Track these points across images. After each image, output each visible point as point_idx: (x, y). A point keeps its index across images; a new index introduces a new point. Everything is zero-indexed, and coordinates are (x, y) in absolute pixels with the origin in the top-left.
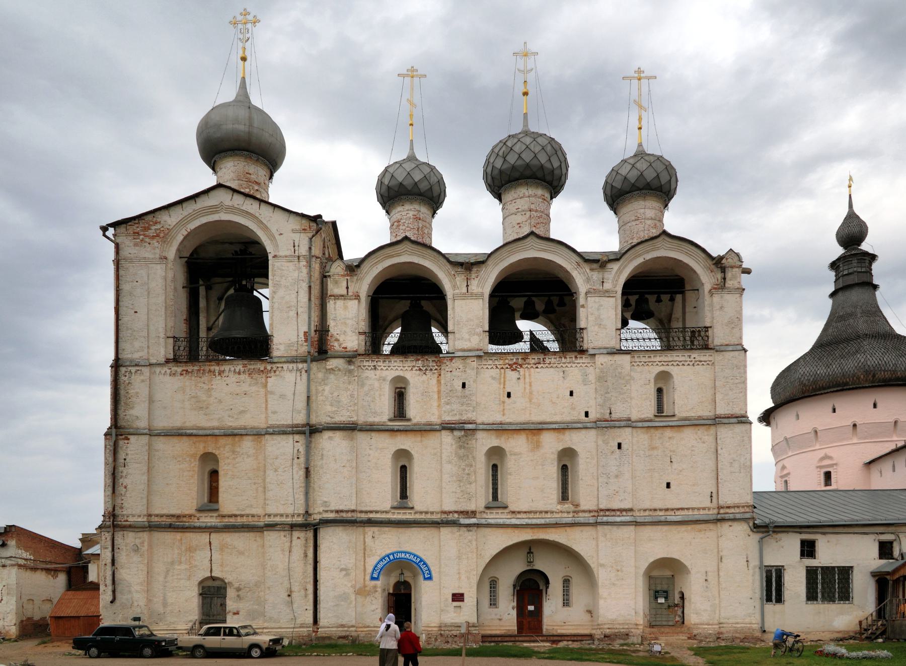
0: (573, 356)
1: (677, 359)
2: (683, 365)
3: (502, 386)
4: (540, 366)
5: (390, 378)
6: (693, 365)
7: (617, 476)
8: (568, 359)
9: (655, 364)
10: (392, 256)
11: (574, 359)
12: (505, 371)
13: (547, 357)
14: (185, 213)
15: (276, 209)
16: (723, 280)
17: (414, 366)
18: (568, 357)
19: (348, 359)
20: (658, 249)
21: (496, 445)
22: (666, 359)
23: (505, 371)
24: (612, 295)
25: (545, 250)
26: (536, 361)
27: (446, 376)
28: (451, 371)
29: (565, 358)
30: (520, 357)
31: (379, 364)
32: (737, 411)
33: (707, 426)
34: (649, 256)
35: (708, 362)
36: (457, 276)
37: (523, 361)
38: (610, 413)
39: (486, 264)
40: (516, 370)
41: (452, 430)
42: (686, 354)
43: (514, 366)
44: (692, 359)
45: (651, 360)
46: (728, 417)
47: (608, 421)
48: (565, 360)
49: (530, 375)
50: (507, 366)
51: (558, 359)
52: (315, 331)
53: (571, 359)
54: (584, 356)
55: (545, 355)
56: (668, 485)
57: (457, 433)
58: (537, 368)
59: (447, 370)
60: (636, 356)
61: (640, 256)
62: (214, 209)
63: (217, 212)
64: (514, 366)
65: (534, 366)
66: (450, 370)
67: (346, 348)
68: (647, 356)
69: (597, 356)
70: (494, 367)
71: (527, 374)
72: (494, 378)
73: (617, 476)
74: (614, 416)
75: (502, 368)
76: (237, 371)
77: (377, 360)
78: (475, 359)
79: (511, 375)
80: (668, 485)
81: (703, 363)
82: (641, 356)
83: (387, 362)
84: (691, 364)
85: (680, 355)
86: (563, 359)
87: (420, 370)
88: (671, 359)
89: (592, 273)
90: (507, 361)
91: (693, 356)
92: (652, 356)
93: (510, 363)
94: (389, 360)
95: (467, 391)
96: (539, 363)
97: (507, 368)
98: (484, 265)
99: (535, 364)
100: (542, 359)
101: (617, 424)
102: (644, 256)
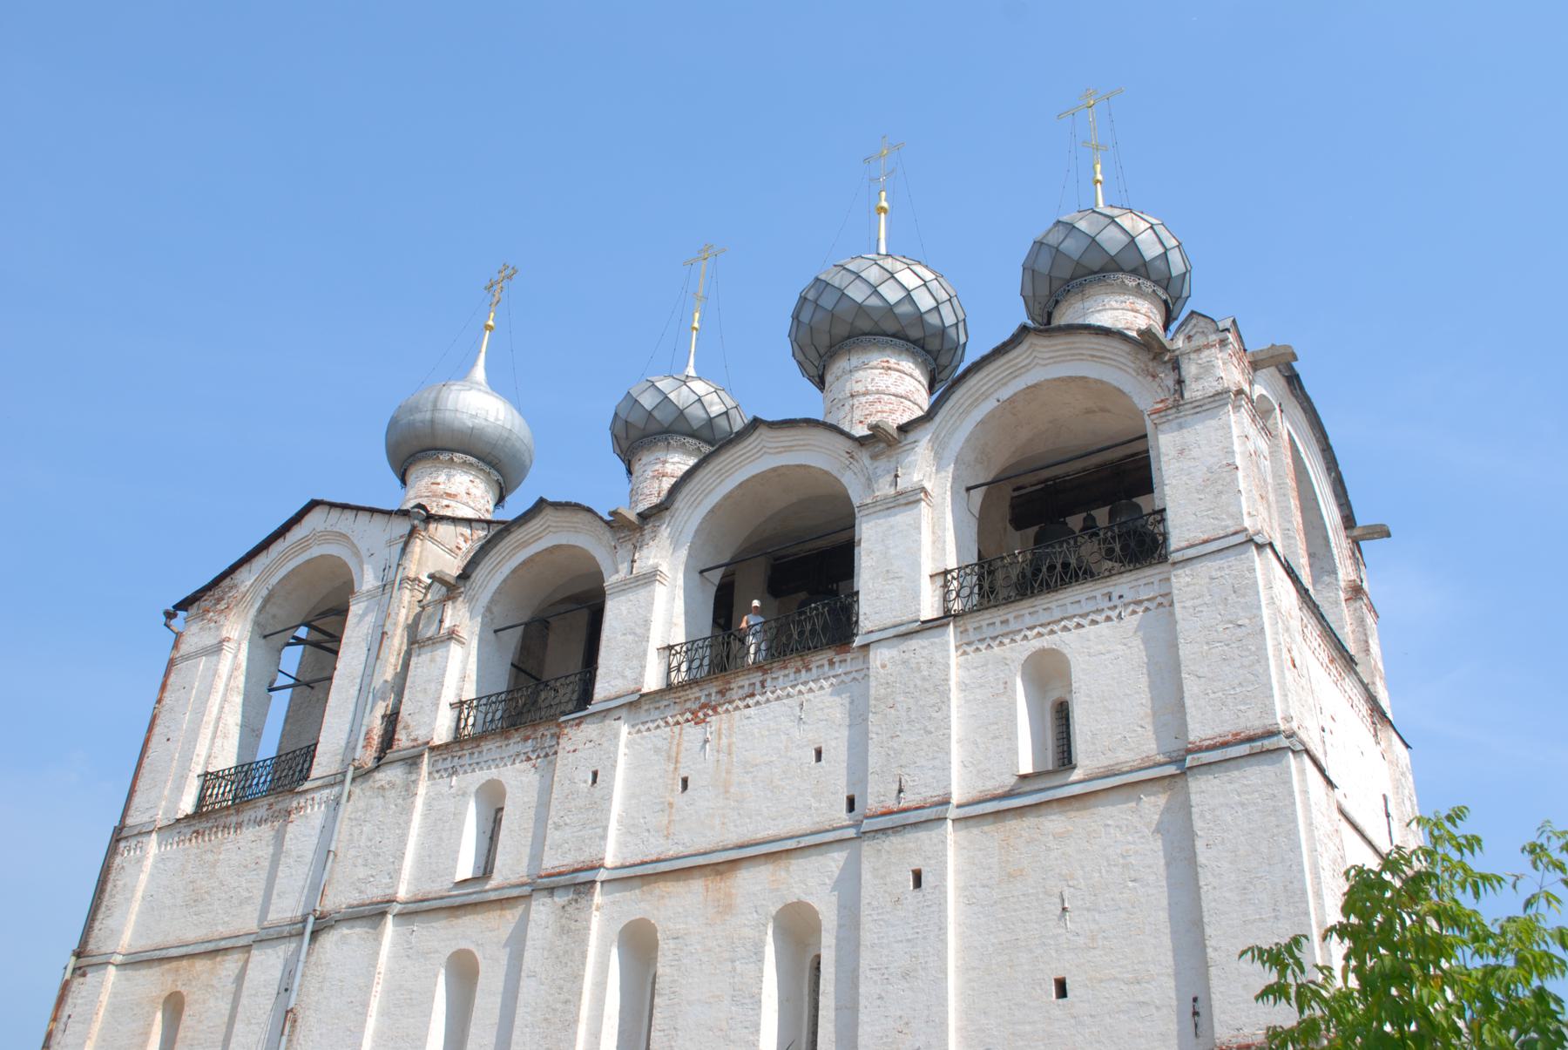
0: (825, 662)
1: (1071, 610)
2: (1094, 622)
3: (672, 766)
4: (750, 701)
5: (473, 789)
6: (1119, 616)
7: (906, 975)
8: (814, 670)
9: (1019, 638)
10: (525, 544)
11: (826, 667)
12: (681, 729)
13: (768, 677)
14: (269, 560)
15: (375, 515)
16: (1177, 387)
17: (518, 755)
18: (813, 666)
19: (410, 761)
20: (1026, 368)
21: (638, 917)
22: (1044, 617)
23: (681, 729)
24: (912, 499)
25: (789, 449)
26: (746, 690)
27: (564, 760)
28: (574, 751)
29: (808, 670)
30: (714, 691)
31: (462, 762)
32: (1252, 722)
33: (1167, 782)
34: (1006, 393)
35: (1160, 600)
36: (618, 548)
37: (719, 696)
38: (900, 791)
39: (673, 509)
40: (704, 721)
41: (551, 890)
42: (1098, 594)
43: (701, 715)
44: (1115, 601)
45: (1008, 630)
46: (1225, 745)
47: (891, 813)
48: (809, 674)
49: (730, 728)
50: (688, 715)
51: (792, 676)
52: (383, 717)
53: (820, 670)
54: (849, 656)
55: (765, 672)
56: (1062, 989)
57: (560, 899)
58: (748, 706)
59: (567, 749)
60: (970, 627)
61: (986, 396)
62: (304, 544)
63: (308, 547)
64: (701, 715)
65: (741, 704)
66: (572, 748)
67: (416, 740)
68: (998, 620)
69: (872, 646)
70: (662, 723)
71: (724, 726)
72: (657, 750)
73: (906, 975)
74: (909, 799)
75: (678, 723)
76: (253, 818)
77: (460, 753)
78: (624, 713)
79: (693, 733)
80: (1062, 989)
81: (1146, 604)
82: (984, 623)
83: (476, 755)
84: (1114, 614)
85: (1083, 598)
86: (803, 672)
87: (529, 759)
88: (1057, 614)
89: (876, 464)
90: (688, 705)
91: (1115, 596)
92: (1011, 617)
93: (695, 706)
94: (479, 749)
95: (598, 791)
96: (752, 695)
97: (688, 721)
98: (667, 513)
99: (744, 699)
100: (758, 685)
101: (913, 817)
102: (996, 396)
